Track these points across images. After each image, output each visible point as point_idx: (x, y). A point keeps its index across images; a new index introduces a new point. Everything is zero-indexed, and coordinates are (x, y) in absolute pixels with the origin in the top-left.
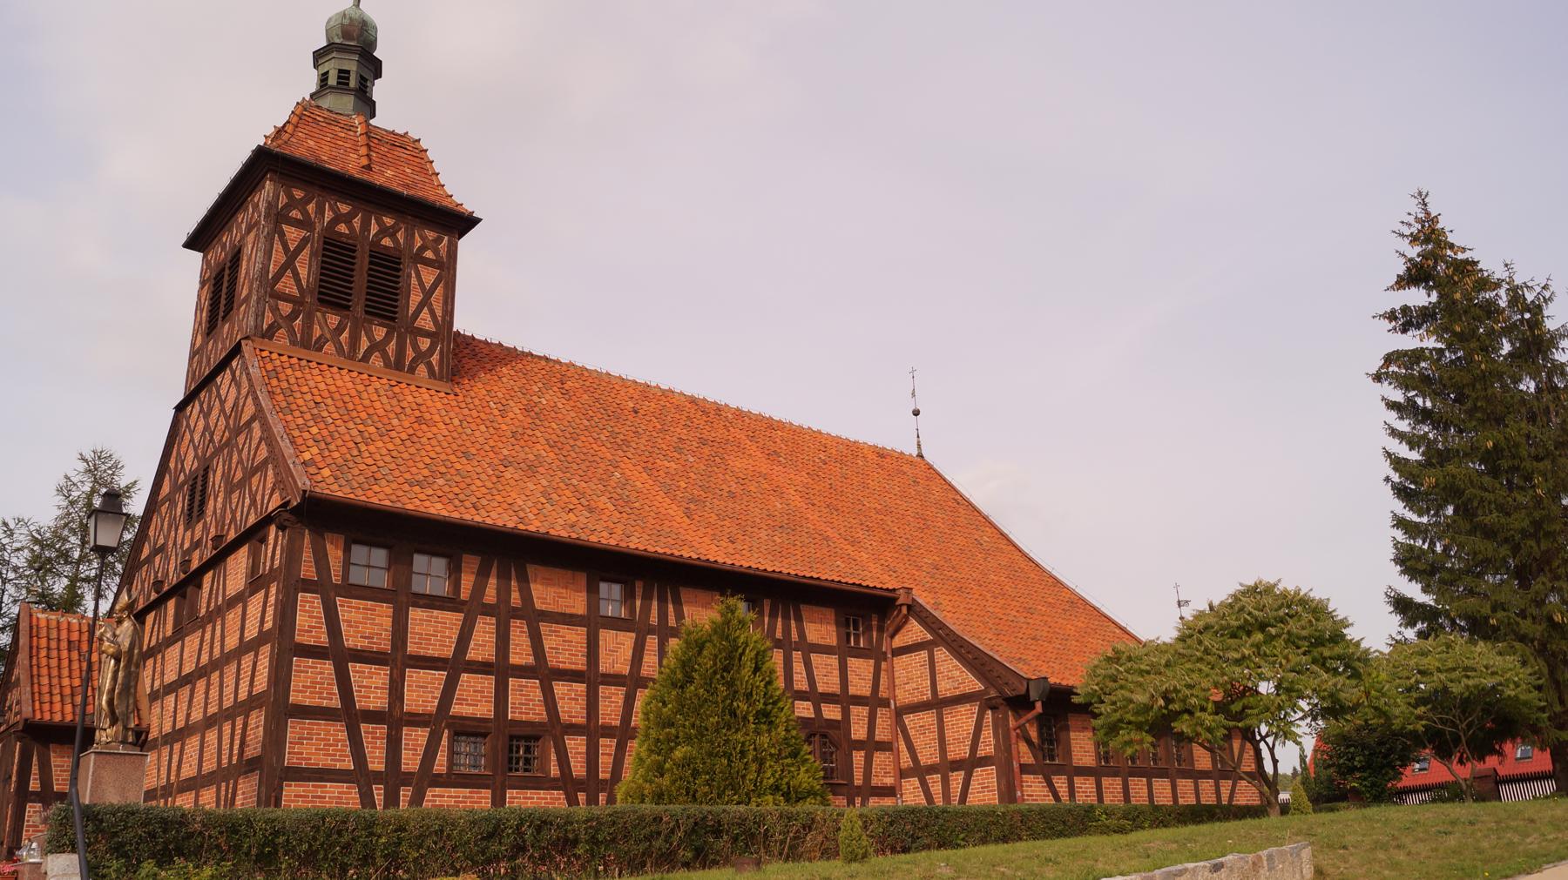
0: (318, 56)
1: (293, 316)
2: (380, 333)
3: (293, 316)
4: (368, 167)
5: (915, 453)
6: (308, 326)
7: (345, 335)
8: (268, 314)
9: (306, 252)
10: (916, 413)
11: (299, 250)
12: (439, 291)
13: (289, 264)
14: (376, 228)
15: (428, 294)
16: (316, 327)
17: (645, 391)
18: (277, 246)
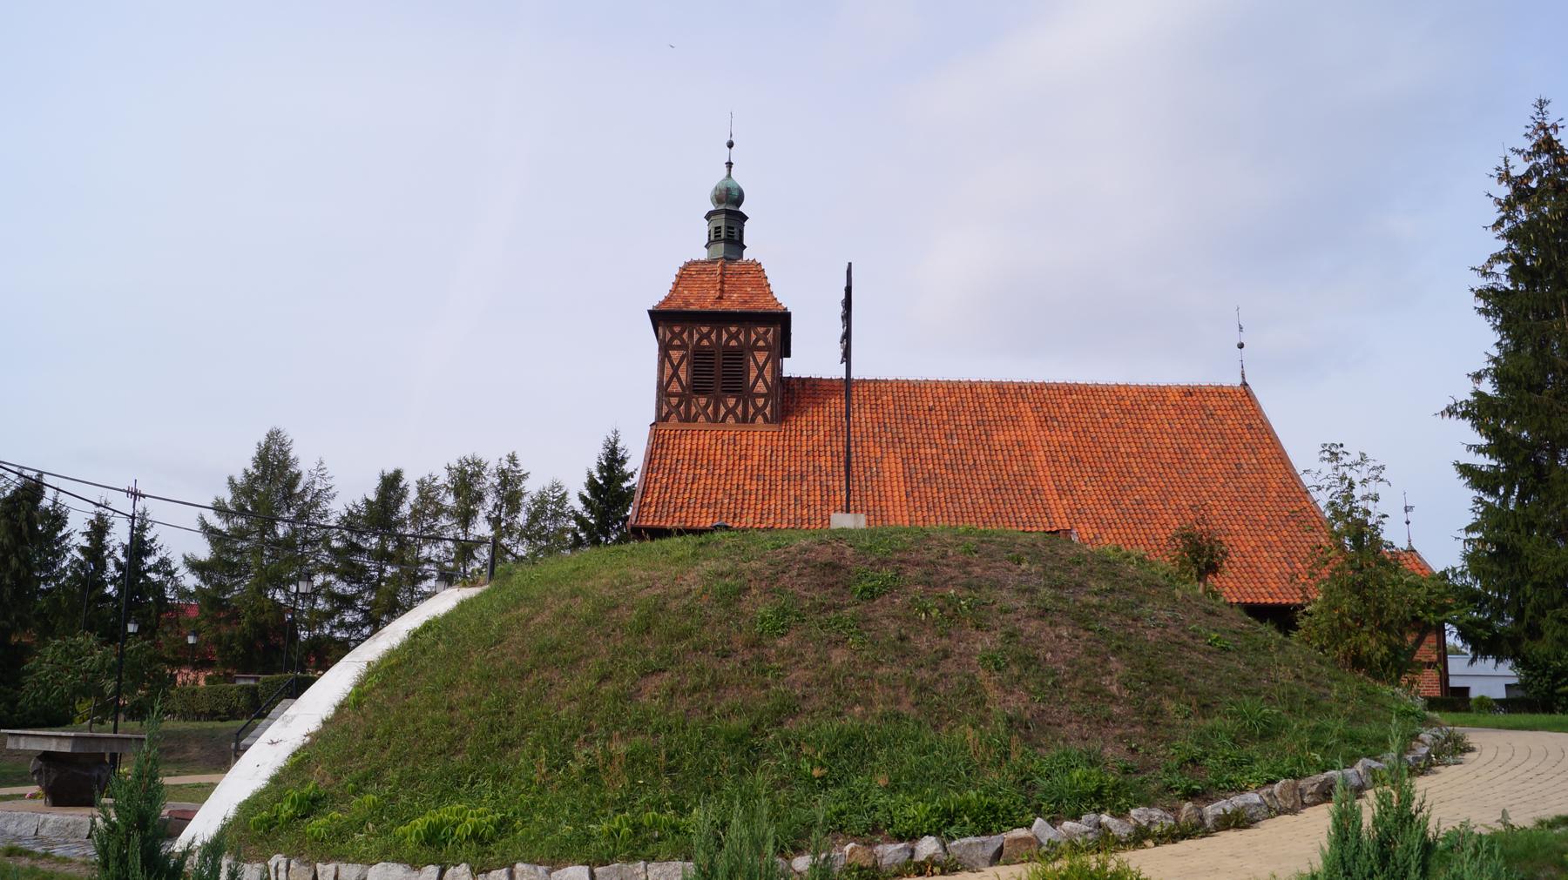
0: (708, 217)
1: (679, 405)
2: (731, 402)
3: (679, 405)
4: (720, 298)
5: (1237, 382)
6: (688, 409)
7: (711, 408)
8: (665, 407)
9: (685, 363)
10: (1241, 346)
11: (680, 363)
12: (769, 365)
13: (675, 374)
14: (728, 337)
15: (761, 369)
16: (693, 408)
17: (952, 388)
18: (667, 365)
